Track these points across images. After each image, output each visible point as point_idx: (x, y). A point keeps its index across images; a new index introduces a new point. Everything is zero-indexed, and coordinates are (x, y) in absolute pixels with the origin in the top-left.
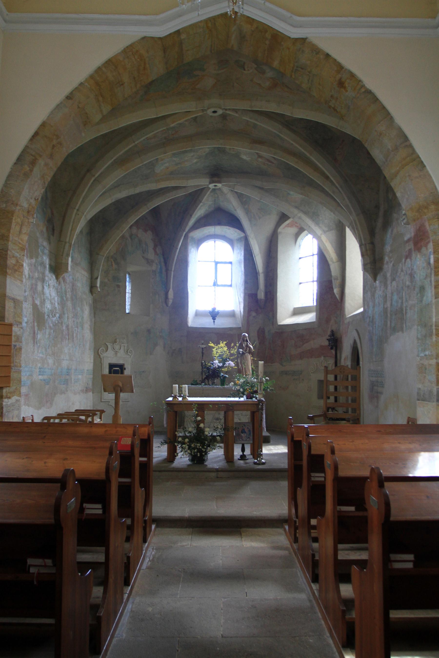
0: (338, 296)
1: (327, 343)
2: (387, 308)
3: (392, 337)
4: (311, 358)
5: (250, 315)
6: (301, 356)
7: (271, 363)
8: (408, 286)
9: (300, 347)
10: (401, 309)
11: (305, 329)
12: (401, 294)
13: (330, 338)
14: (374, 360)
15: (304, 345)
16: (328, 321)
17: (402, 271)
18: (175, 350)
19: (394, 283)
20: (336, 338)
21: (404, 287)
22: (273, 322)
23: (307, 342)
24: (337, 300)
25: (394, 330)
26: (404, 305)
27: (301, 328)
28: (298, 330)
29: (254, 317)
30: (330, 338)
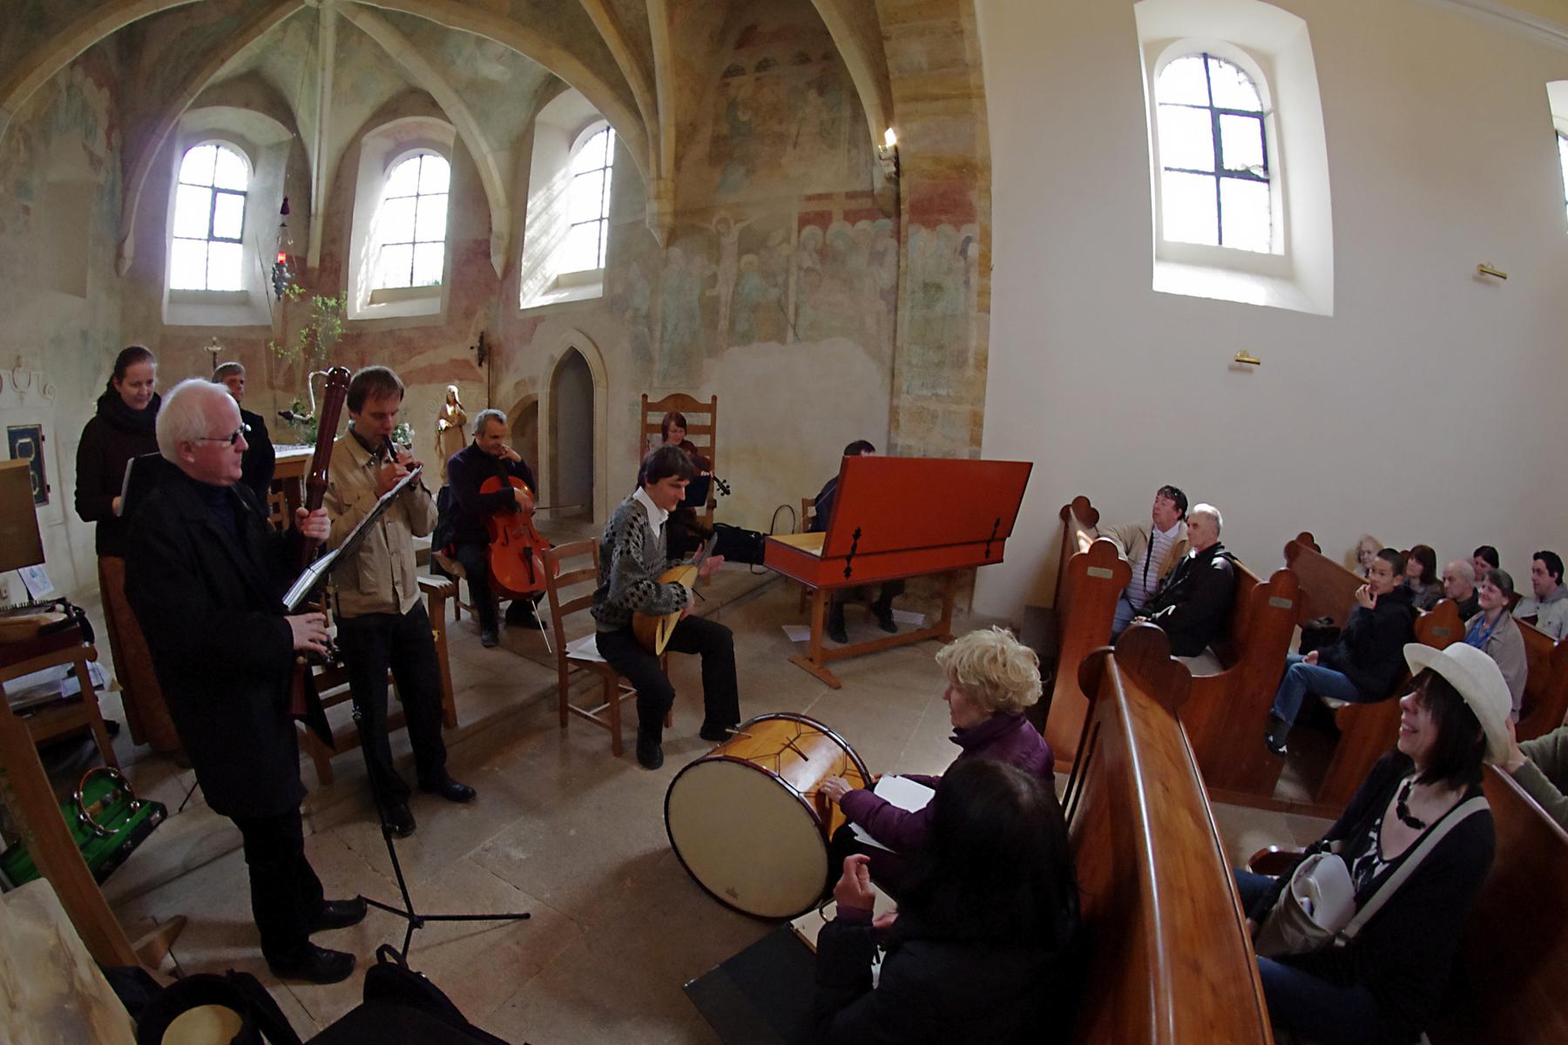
0: (499, 271)
1: (472, 356)
2: (716, 299)
3: (736, 349)
4: (429, 382)
8: (809, 270)
10: (782, 308)
12: (780, 280)
15: (413, 359)
16: (469, 314)
17: (787, 240)
19: (747, 258)
21: (794, 269)
23: (421, 353)
25: (746, 339)
26: (792, 299)
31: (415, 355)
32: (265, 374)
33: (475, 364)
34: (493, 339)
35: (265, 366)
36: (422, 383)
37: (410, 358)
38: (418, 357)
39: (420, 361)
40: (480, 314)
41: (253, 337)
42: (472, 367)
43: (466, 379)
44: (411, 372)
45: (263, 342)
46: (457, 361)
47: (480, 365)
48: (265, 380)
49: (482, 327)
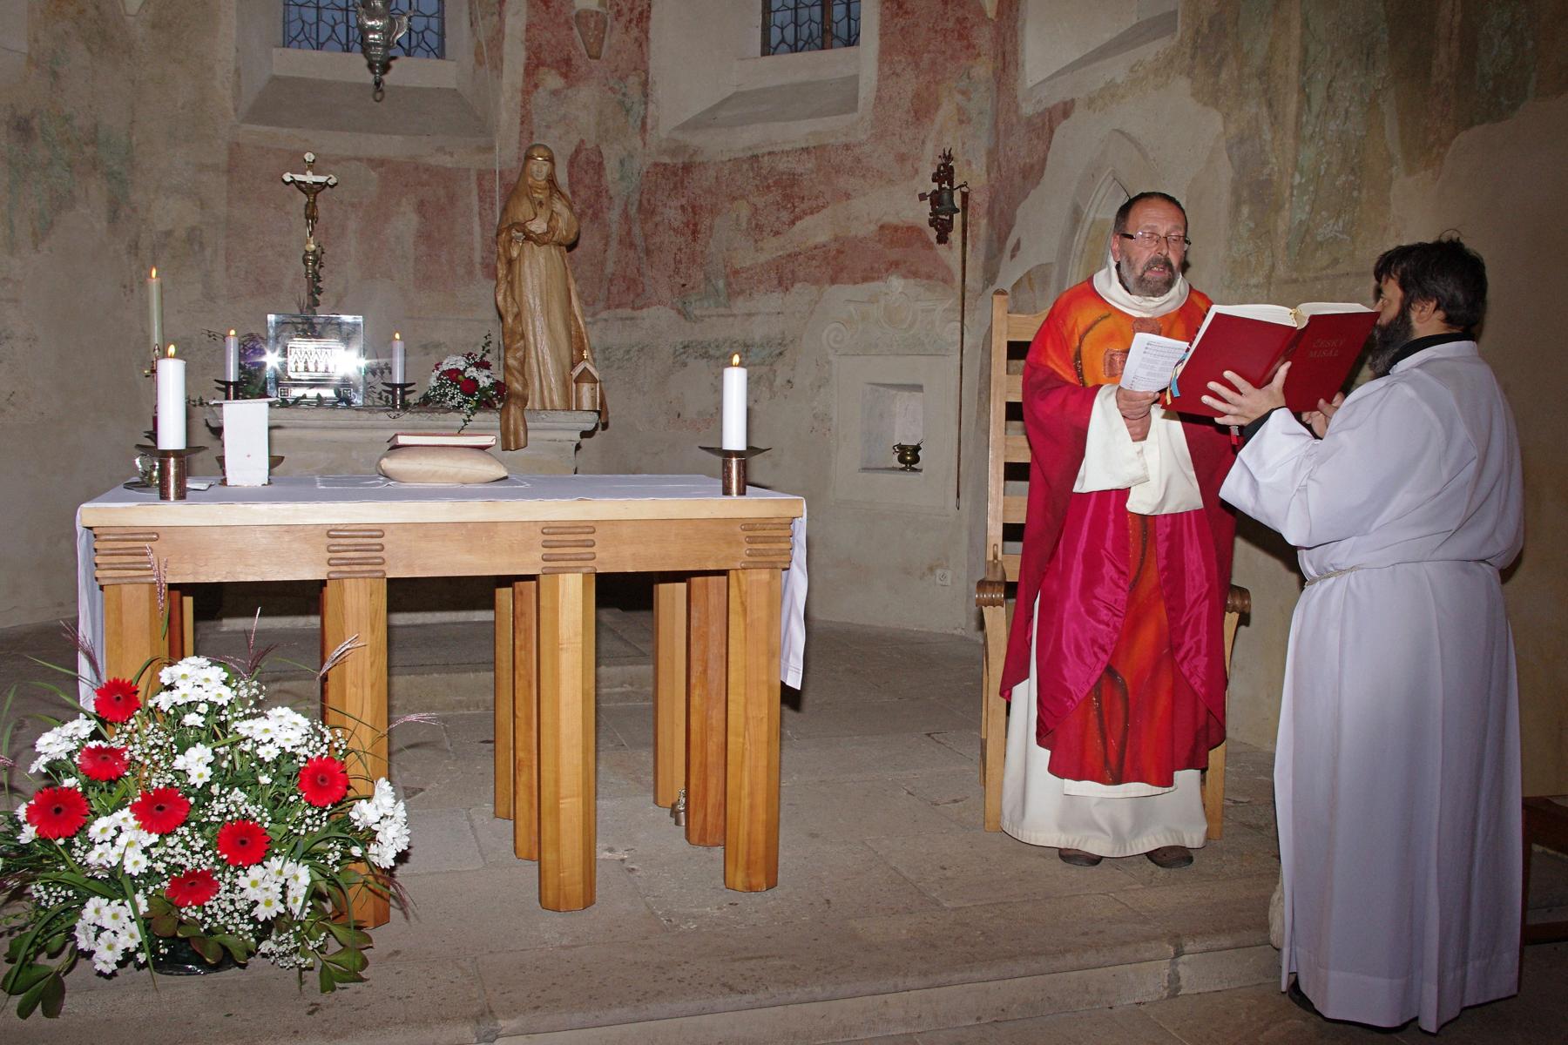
4: (833, 281)
5: (536, 86)
6: (783, 276)
7: (633, 308)
9: (777, 233)
11: (806, 150)
13: (935, 186)
14: (1281, 271)
16: (922, 110)
18: (169, 234)
20: (965, 189)
22: (644, 124)
24: (981, 12)
27: (787, 147)
28: (770, 153)
29: (555, 93)
30: (935, 186)
31: (805, 213)
32: (478, 245)
33: (932, 234)
34: (973, 174)
35: (477, 229)
36: (817, 282)
37: (793, 223)
38: (808, 218)
39: (816, 230)
40: (946, 110)
41: (447, 161)
42: (929, 245)
43: (915, 274)
44: (792, 257)
45: (474, 178)
46: (896, 229)
47: (942, 239)
48: (477, 257)
49: (950, 142)
